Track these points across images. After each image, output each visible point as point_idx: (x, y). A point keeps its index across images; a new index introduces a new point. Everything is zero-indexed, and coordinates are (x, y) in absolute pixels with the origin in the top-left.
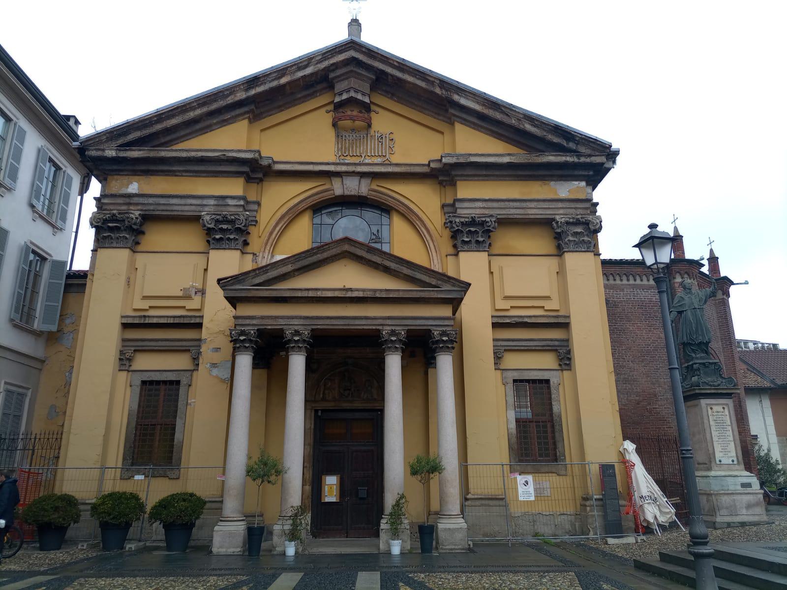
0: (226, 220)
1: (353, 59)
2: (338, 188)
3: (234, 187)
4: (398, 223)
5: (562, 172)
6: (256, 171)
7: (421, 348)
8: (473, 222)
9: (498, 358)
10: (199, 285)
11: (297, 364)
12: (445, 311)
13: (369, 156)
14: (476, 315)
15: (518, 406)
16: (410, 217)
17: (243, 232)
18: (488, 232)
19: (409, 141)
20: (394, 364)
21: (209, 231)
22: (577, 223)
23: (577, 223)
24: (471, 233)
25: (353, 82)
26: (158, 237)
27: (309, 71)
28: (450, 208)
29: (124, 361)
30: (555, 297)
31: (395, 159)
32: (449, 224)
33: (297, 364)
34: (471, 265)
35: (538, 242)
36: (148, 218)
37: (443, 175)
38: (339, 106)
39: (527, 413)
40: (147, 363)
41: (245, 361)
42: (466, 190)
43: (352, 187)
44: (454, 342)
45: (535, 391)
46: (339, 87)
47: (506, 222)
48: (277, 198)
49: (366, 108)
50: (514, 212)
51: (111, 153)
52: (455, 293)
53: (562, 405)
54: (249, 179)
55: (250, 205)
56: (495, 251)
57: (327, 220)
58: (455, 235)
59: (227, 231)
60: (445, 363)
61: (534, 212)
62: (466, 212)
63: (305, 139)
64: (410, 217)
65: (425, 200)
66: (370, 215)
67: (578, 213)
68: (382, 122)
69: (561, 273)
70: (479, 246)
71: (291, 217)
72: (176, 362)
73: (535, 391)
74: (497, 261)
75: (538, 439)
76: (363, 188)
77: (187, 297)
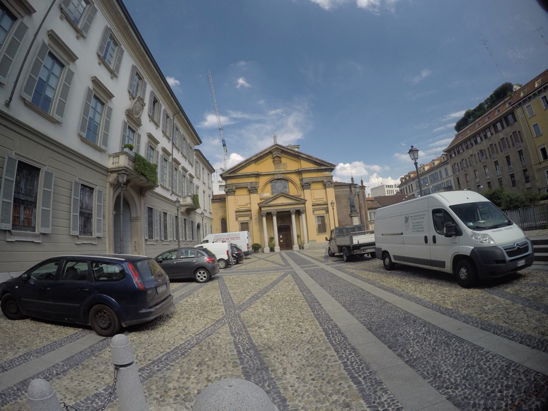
0: (253, 187)
1: (276, 148)
2: (276, 177)
3: (253, 180)
4: (290, 184)
5: (325, 170)
6: (257, 175)
7: (298, 213)
8: (306, 183)
9: (313, 212)
10: (249, 202)
11: (275, 218)
12: (303, 206)
14: (309, 206)
15: (319, 221)
16: (292, 182)
17: (256, 190)
18: (310, 185)
19: (291, 165)
20: (293, 217)
21: (249, 190)
22: (328, 182)
23: (328, 182)
24: (305, 186)
25: (276, 152)
26: (238, 192)
27: (267, 152)
28: (301, 180)
29: (237, 219)
30: (325, 198)
31: (288, 169)
32: (301, 184)
33: (275, 218)
34: (307, 192)
35: (320, 186)
37: (299, 173)
38: (273, 158)
39: (320, 223)
40: (240, 219)
41: (264, 219)
42: (305, 176)
43: (279, 176)
44: (305, 211)
45: (322, 218)
46: (274, 153)
48: (263, 181)
49: (280, 158)
50: (315, 180)
51: (228, 175)
52: (304, 202)
53: (327, 221)
54: (256, 177)
55: (257, 183)
56: (312, 188)
57: (274, 184)
58: (303, 186)
59: (253, 190)
60: (303, 216)
61: (319, 180)
62: (305, 181)
63: (267, 166)
64: (292, 182)
65: (295, 178)
66: (283, 182)
67: (329, 179)
68: (284, 160)
69: (326, 192)
70: (308, 188)
71: (266, 184)
72: (246, 219)
73: (322, 218)
74: (313, 191)
76: (281, 176)
77: (247, 205)
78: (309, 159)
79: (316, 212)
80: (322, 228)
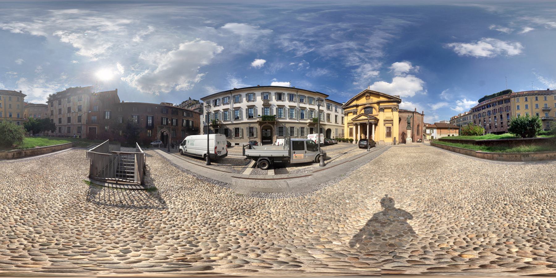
3: (355, 108)
6: (357, 106)
11: (359, 127)
13: (370, 101)
16: (375, 108)
24: (382, 110)
26: (349, 114)
33: (359, 127)
36: (348, 113)
37: (378, 103)
42: (381, 104)
45: (389, 128)
47: (386, 108)
53: (392, 130)
62: (381, 107)
64: (375, 108)
73: (389, 128)
75: (389, 134)
76: (369, 105)
78: (384, 96)
79: (386, 125)
80: (389, 134)
